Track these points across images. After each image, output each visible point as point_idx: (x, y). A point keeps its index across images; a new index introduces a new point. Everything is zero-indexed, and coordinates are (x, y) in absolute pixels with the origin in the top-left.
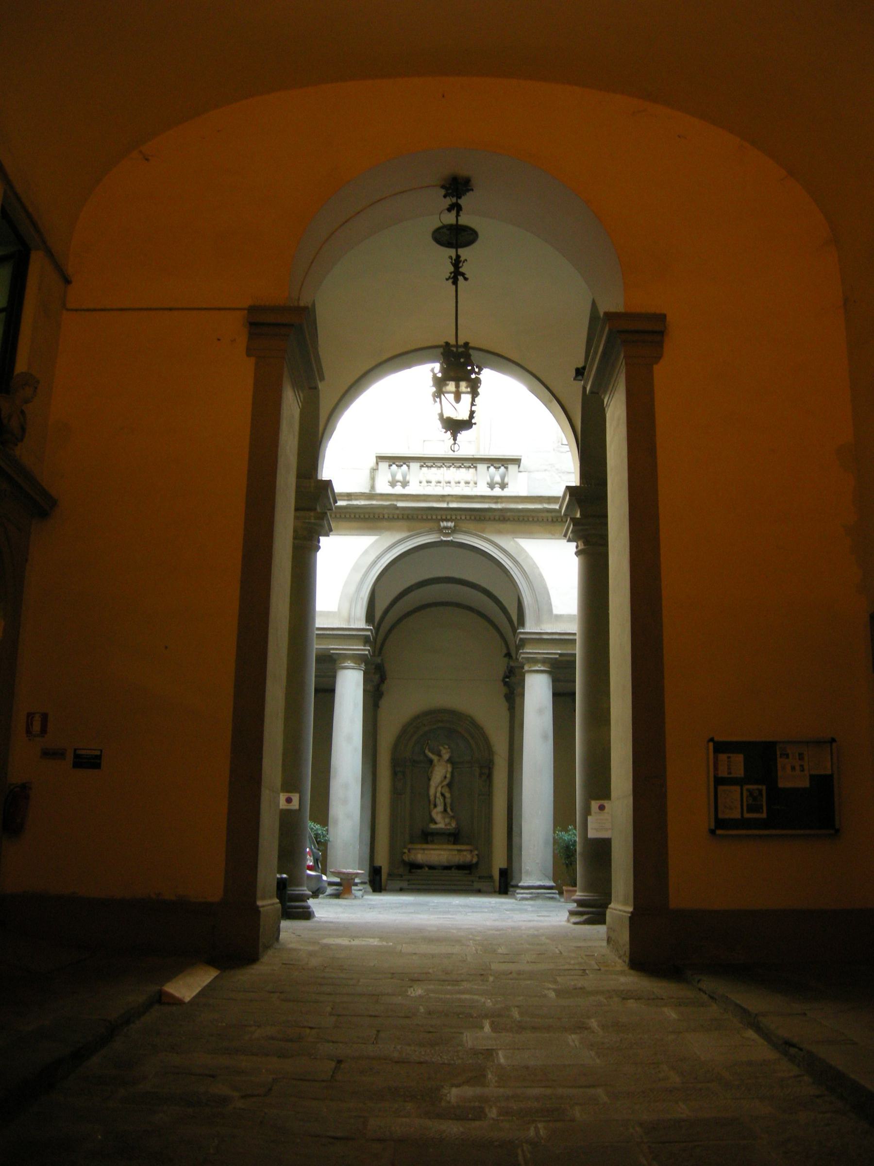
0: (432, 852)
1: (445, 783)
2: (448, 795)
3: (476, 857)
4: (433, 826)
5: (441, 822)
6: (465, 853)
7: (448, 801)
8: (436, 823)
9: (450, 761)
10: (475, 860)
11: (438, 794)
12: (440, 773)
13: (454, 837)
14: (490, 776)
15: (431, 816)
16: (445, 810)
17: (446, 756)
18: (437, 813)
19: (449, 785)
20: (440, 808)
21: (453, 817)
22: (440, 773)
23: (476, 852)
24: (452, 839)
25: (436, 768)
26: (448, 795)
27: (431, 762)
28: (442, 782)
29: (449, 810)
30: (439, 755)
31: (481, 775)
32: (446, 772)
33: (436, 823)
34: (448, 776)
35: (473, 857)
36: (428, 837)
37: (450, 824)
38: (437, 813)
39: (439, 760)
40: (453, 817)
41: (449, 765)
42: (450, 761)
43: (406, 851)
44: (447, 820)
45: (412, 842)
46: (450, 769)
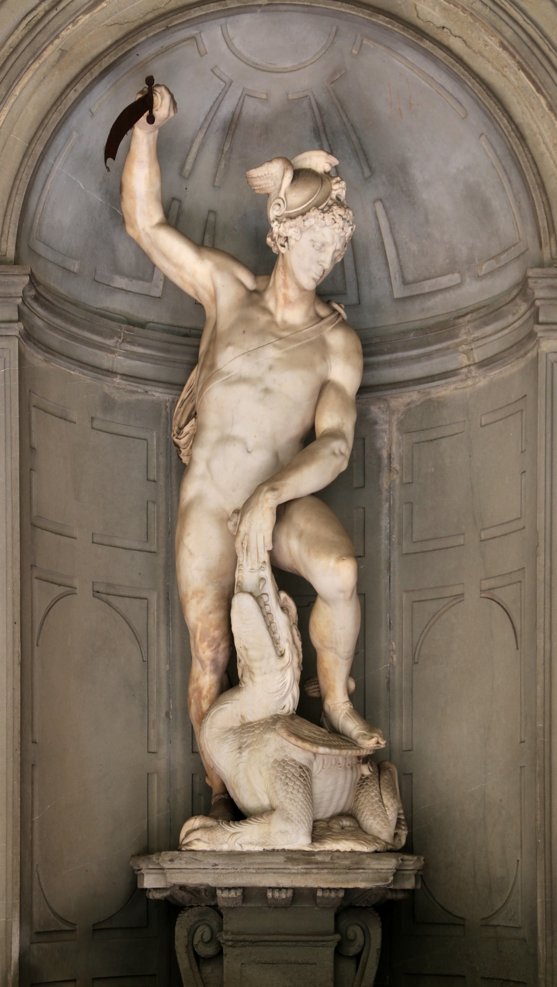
1: (311, 478)
2: (333, 576)
4: (203, 837)
7: (336, 625)
8: (234, 813)
11: (254, 571)
15: (194, 749)
16: (310, 708)
18: (246, 731)
19: (345, 505)
20: (271, 686)
26: (333, 576)
28: (279, 470)
30: (262, 260)
33: (236, 814)
34: (334, 418)
37: (347, 820)
41: (337, 339)
46: (345, 374)
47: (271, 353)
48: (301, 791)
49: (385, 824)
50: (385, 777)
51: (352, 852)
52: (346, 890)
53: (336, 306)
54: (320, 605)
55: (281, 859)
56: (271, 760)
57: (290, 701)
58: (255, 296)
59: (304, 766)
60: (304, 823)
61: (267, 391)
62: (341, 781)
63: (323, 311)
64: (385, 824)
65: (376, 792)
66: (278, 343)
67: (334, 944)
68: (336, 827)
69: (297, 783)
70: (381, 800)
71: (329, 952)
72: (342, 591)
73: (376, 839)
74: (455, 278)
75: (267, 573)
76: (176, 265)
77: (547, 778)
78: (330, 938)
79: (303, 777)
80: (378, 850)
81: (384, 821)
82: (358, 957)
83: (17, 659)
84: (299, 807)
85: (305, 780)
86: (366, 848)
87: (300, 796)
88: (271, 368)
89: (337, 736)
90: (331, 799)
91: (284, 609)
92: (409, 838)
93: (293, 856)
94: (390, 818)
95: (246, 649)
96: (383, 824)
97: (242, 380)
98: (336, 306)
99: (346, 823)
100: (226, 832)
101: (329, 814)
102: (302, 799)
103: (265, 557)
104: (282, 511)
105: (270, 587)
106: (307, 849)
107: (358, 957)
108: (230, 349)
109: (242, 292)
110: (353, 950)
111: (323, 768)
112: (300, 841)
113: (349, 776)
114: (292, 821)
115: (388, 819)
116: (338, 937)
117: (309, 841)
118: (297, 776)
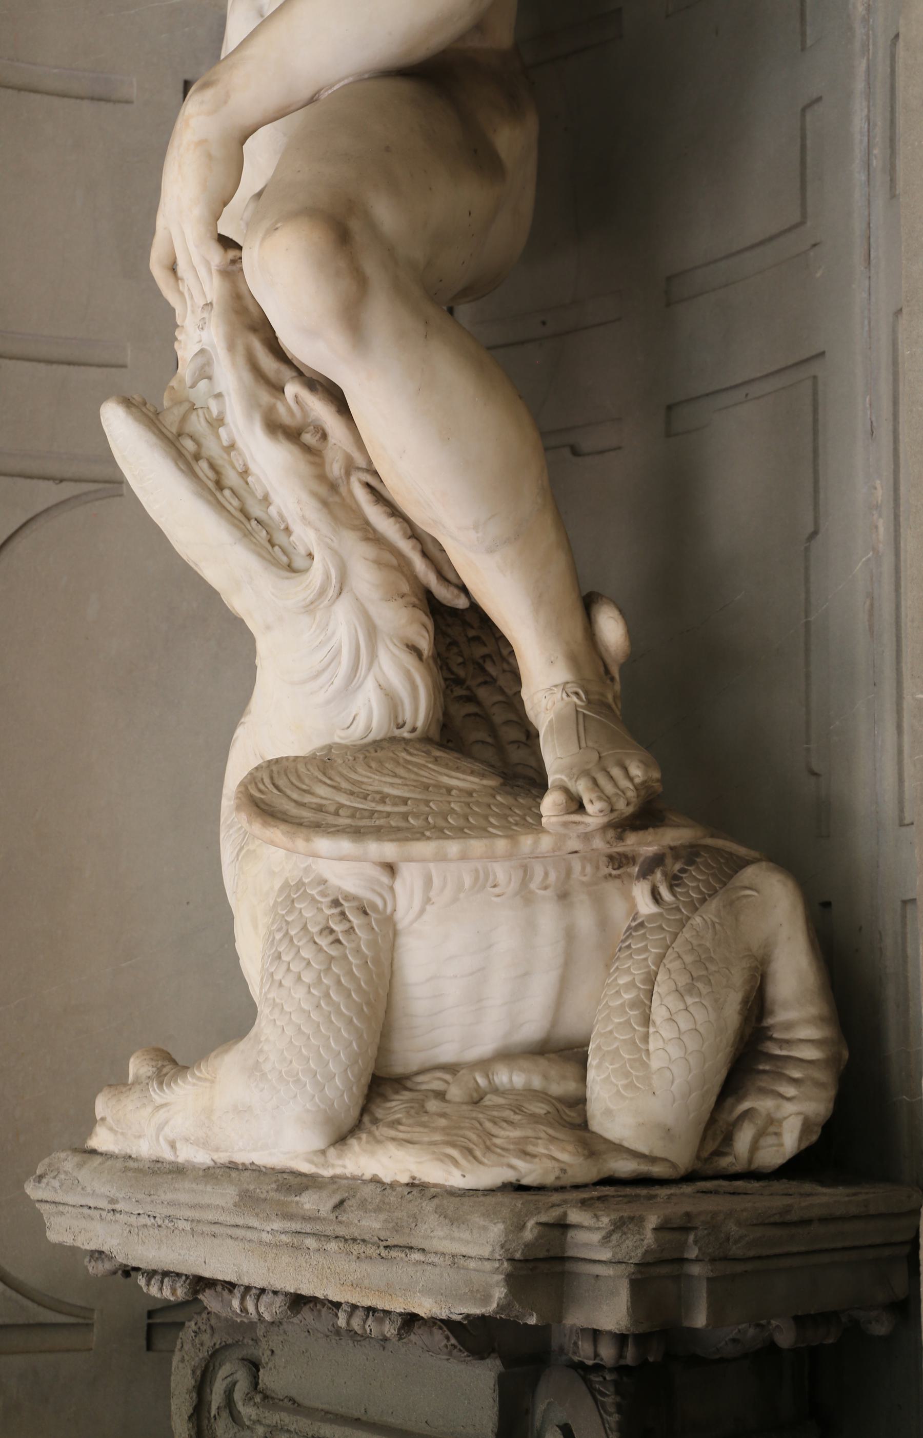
48: (307, 978)
49: (630, 1086)
51: (416, 1187)
55: (224, 1195)
56: (277, 884)
59: (349, 897)
60: (297, 1081)
62: (506, 940)
64: (630, 1086)
69: (306, 953)
79: (332, 931)
80: (525, 1182)
81: (627, 1075)
84: (289, 1031)
85: (338, 941)
86: (457, 1173)
87: (299, 993)
93: (272, 1190)
94: (655, 1063)
96: (621, 1083)
102: (305, 1006)
106: (305, 1167)
111: (427, 901)
114: (264, 1075)
115: (645, 1065)
117: (318, 1142)
118: (314, 929)
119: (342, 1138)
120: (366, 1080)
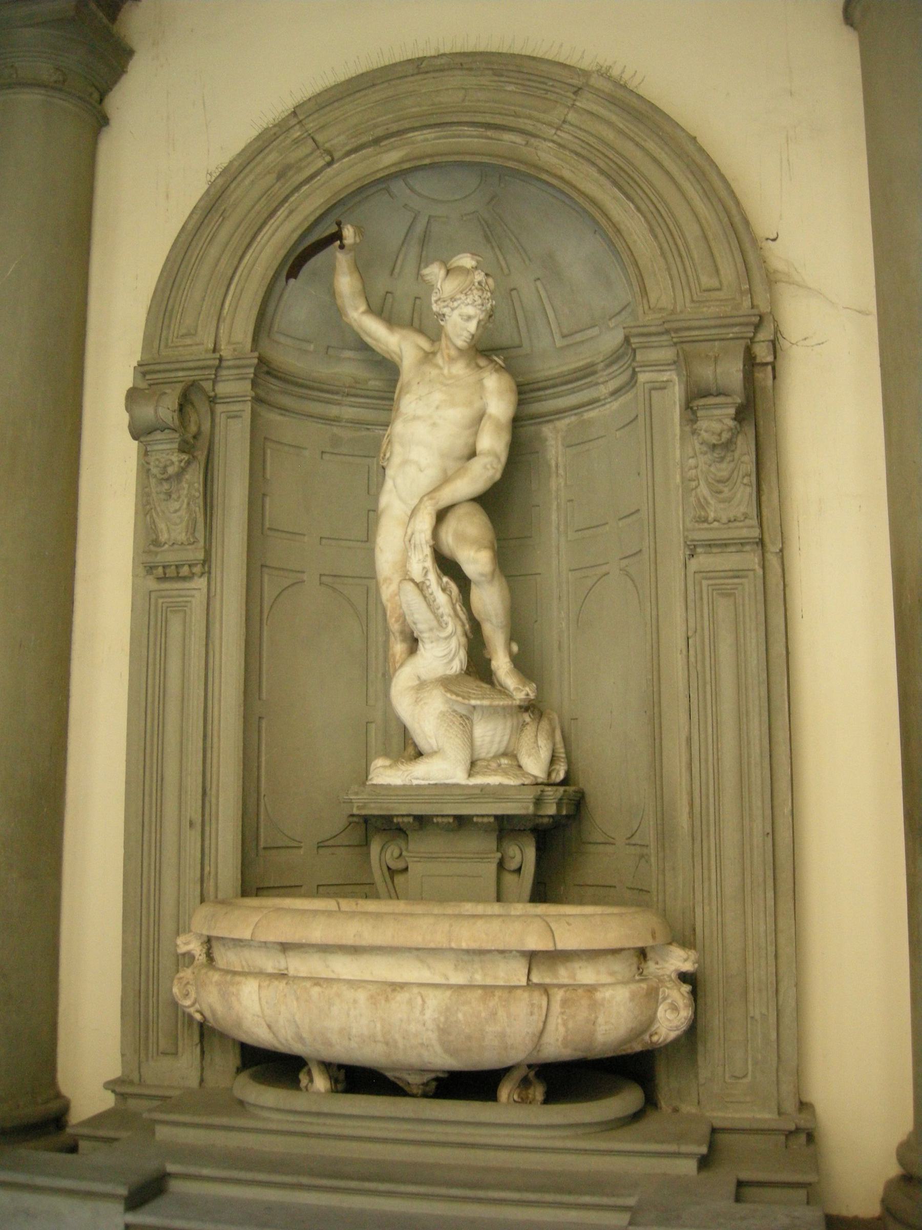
0: (344, 967)
3: (679, 994)
5: (448, 746)
6: (586, 974)
9: (485, 350)
10: (670, 1022)
12: (439, 431)
13: (550, 846)
14: (754, 410)
17: (462, 318)
21: (533, 708)
22: (439, 431)
23: (679, 960)
24: (524, 854)
25: (410, 404)
26: (476, 561)
27: (388, 369)
29: (501, 664)
31: (696, 397)
32: (480, 418)
35: (652, 996)
36: (380, 847)
38: (421, 689)
39: (428, 357)
40: (533, 708)
42: (485, 350)
43: (191, 945)
44: (489, 734)
45: (252, 885)
47: (438, 396)
50: (545, 724)
52: (496, 817)
53: (496, 359)
54: (473, 587)
57: (457, 665)
58: (431, 356)
61: (434, 425)
63: (482, 362)
65: (533, 735)
66: (444, 388)
67: (497, 861)
68: (494, 765)
70: (536, 742)
71: (493, 867)
72: (482, 575)
73: (526, 774)
74: (595, 331)
75: (429, 563)
76: (375, 339)
77: (656, 721)
78: (492, 855)
82: (519, 870)
83: (243, 638)
88: (437, 408)
89: (504, 691)
90: (492, 742)
91: (444, 590)
92: (567, 773)
95: (415, 623)
97: (415, 418)
98: (496, 359)
99: (504, 761)
100: (399, 769)
101: (491, 755)
103: (428, 551)
104: (441, 516)
105: (432, 577)
107: (519, 870)
108: (408, 396)
109: (421, 354)
110: (514, 865)
112: (459, 776)
113: (509, 724)
116: (499, 855)
117: (466, 776)
119: (470, 775)
120: (469, 762)
